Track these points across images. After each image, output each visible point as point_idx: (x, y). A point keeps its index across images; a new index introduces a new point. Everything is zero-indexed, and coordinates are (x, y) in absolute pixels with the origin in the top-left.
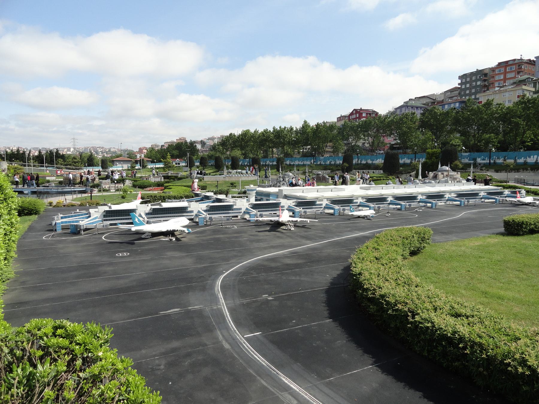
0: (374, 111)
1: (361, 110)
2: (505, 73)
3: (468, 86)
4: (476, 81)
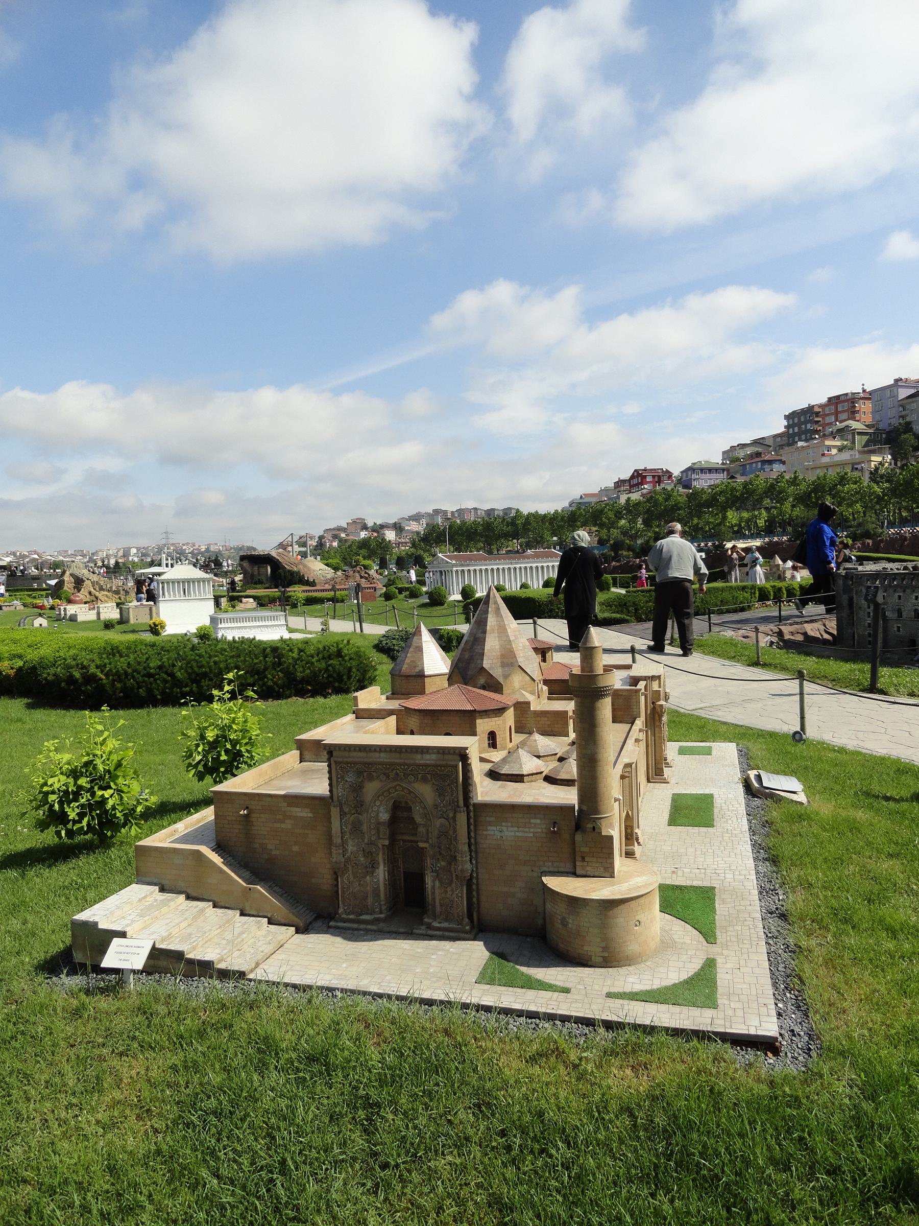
0: (667, 471)
1: (645, 470)
2: (837, 413)
3: (796, 430)
4: (806, 422)
